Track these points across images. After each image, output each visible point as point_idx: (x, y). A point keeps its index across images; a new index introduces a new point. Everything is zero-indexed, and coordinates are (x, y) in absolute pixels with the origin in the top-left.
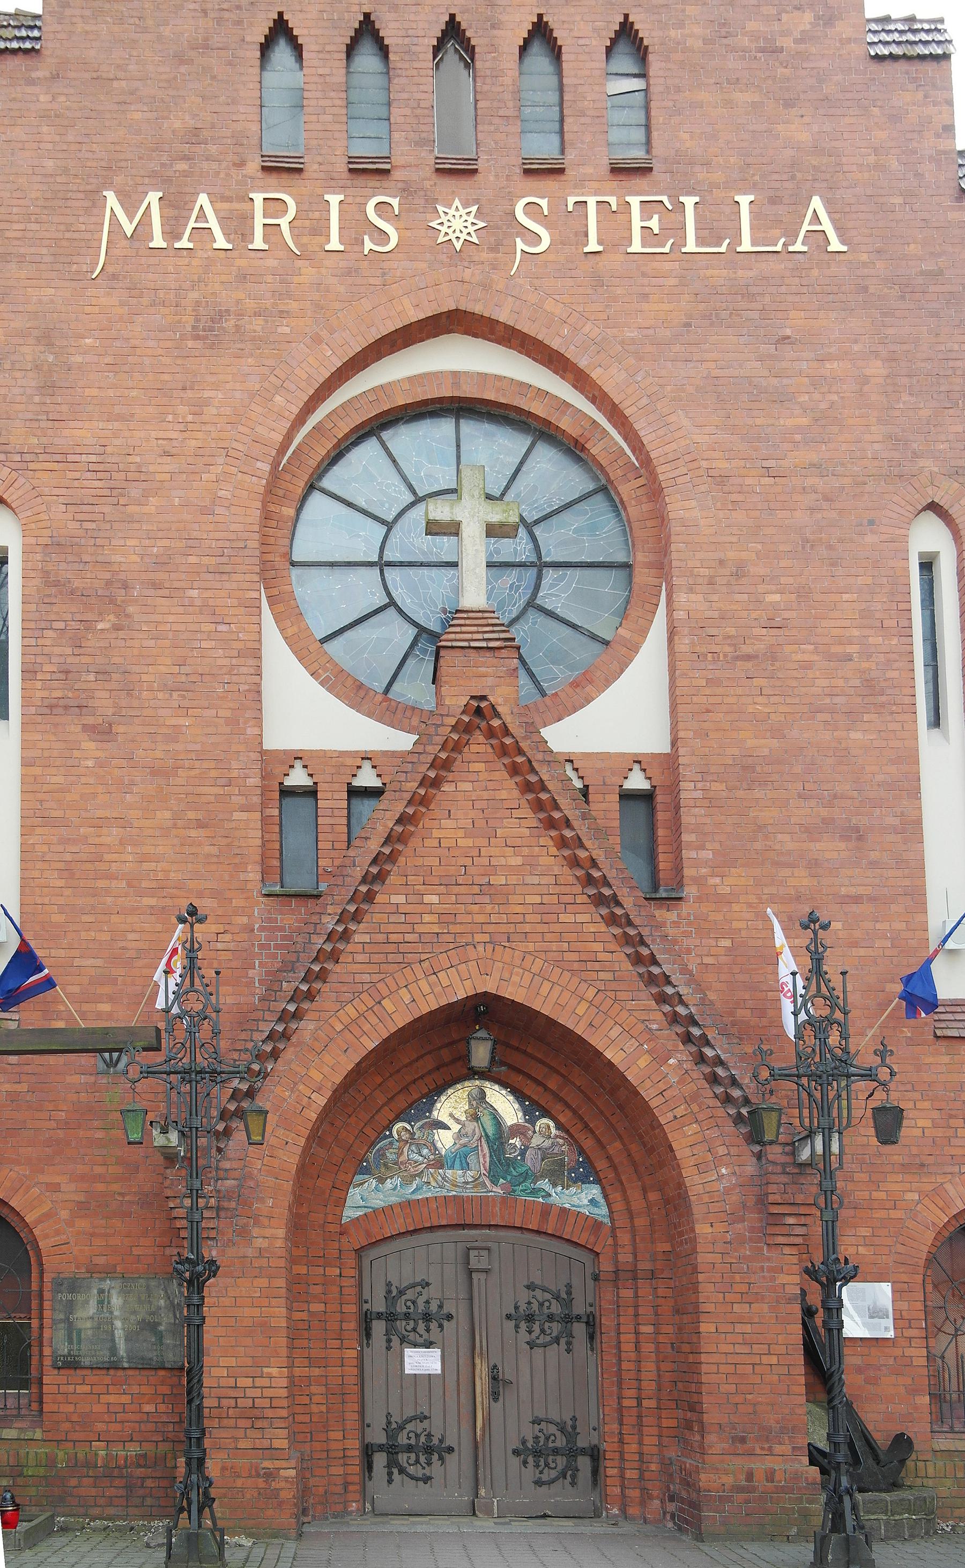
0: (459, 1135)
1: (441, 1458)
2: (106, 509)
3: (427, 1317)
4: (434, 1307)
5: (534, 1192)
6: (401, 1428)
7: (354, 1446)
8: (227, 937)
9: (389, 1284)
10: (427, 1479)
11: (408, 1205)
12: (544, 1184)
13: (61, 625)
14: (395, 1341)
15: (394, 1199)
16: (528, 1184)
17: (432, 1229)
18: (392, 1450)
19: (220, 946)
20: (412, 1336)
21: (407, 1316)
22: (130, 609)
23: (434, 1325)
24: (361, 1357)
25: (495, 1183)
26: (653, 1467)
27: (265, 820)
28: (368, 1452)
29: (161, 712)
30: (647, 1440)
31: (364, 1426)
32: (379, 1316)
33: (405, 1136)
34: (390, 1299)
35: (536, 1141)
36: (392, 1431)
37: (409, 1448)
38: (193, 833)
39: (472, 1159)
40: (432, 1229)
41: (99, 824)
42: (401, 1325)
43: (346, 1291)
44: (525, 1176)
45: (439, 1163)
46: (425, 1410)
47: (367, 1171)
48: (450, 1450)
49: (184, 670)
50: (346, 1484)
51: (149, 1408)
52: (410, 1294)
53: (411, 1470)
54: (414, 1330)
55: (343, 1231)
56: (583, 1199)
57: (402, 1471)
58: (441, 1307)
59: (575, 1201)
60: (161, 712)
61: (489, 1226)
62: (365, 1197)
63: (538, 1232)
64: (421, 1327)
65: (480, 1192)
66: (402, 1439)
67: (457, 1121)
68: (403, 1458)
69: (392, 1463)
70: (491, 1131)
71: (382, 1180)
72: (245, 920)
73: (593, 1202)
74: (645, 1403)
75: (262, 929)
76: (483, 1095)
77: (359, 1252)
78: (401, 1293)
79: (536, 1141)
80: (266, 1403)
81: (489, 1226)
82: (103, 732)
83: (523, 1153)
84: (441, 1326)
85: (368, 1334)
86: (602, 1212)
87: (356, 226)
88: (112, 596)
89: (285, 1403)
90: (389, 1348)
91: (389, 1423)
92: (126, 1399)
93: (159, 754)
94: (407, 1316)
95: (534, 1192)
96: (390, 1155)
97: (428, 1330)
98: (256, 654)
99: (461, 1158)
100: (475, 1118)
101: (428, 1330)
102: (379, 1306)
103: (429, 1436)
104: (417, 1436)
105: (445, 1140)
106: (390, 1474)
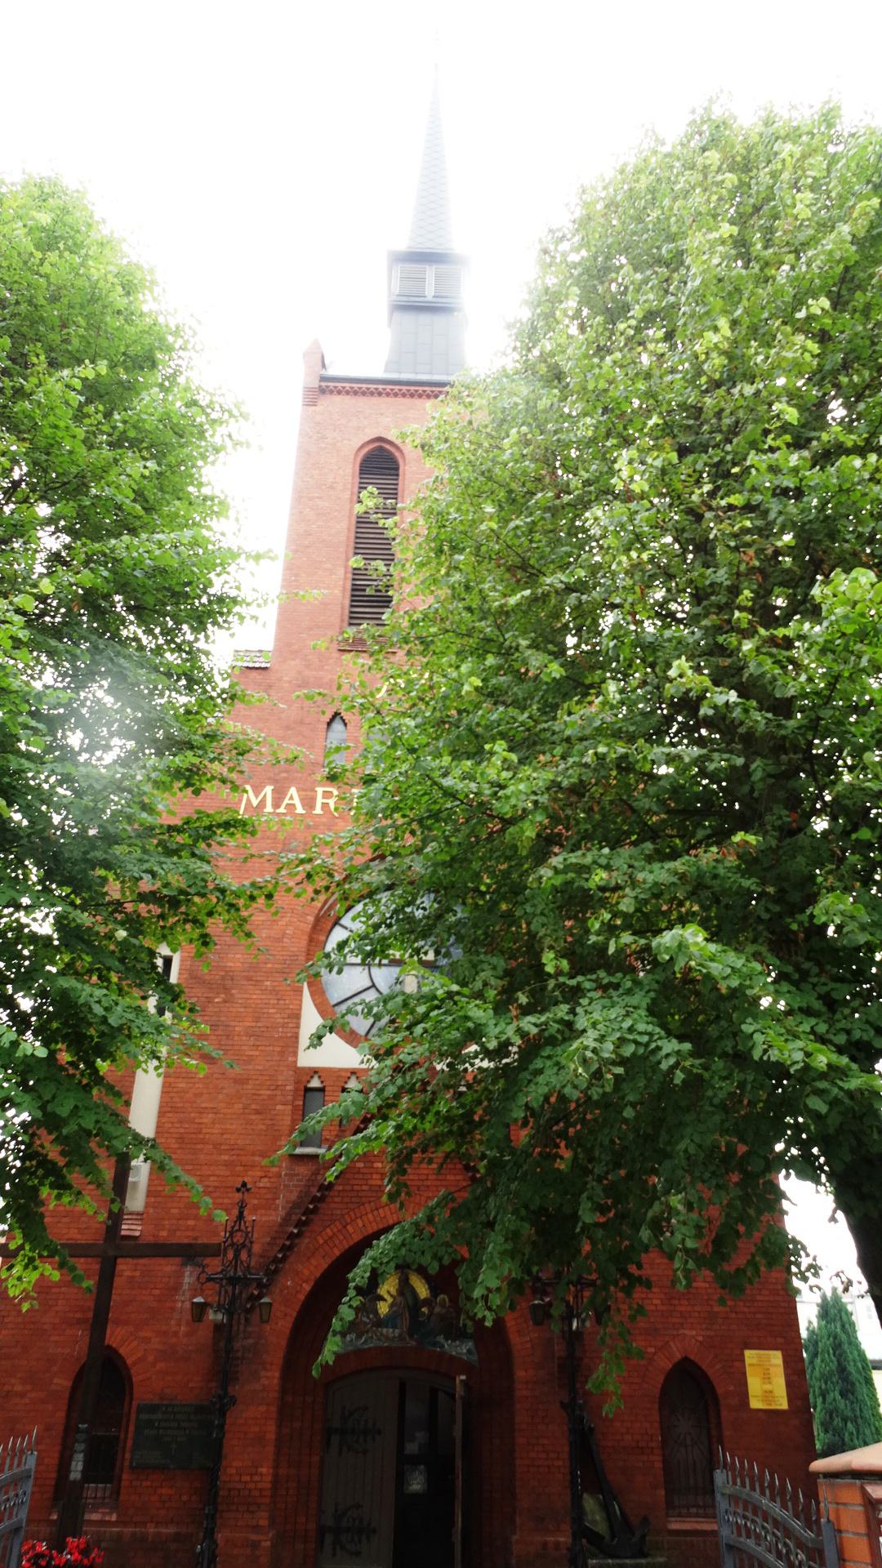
0: (391, 1306)
5: (435, 1344)
10: (358, 1554)
11: (359, 1353)
12: (441, 1339)
25: (411, 1336)
27: (295, 1108)
28: (322, 1531)
35: (437, 1309)
45: (380, 1323)
48: (374, 1531)
70: (410, 1302)
76: (407, 1279)
79: (437, 1309)
80: (257, 1493)
86: (474, 1358)
89: (268, 1493)
99: (392, 1320)
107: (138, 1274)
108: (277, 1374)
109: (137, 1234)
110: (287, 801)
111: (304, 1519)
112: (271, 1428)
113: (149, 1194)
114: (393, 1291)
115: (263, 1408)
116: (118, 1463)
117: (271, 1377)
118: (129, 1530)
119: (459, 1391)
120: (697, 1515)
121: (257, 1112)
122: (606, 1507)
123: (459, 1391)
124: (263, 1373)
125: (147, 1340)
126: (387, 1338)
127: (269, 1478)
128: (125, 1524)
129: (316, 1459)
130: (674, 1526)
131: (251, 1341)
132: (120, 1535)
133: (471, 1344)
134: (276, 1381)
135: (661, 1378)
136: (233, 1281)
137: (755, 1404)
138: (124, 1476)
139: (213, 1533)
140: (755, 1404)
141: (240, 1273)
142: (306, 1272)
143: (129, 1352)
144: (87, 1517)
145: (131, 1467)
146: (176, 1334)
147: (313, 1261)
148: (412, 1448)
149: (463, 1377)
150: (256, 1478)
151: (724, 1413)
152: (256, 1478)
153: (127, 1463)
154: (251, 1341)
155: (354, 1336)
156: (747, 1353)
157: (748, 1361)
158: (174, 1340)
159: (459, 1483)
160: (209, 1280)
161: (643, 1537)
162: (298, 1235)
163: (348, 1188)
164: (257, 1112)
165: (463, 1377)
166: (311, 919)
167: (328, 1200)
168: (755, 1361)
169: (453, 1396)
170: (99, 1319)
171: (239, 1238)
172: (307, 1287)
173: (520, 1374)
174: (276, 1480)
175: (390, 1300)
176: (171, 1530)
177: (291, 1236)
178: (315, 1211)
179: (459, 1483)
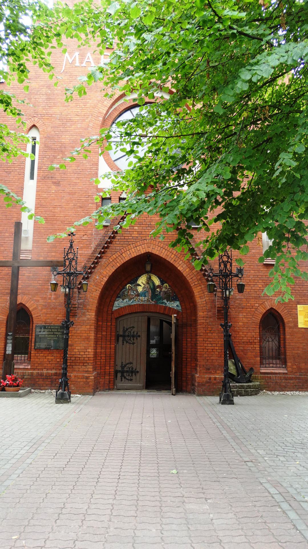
0: (144, 288)
1: (135, 374)
2: (61, 128)
3: (133, 336)
4: (135, 333)
5: (163, 303)
6: (125, 366)
7: (112, 370)
8: (86, 236)
9: (124, 327)
10: (131, 380)
11: (130, 306)
12: (165, 301)
13: (48, 157)
14: (125, 342)
15: (126, 305)
16: (161, 301)
17: (136, 313)
18: (122, 372)
19: (84, 238)
20: (129, 341)
21: (128, 336)
22: (66, 153)
23: (135, 338)
24: (115, 347)
25: (152, 300)
26: (189, 377)
28: (116, 372)
29: (72, 179)
30: (188, 369)
31: (115, 365)
32: (121, 336)
33: (130, 288)
34: (124, 331)
35: (163, 289)
36: (123, 367)
37: (127, 372)
38: (79, 209)
39: (147, 294)
40: (136, 313)
41: (55, 207)
42: (127, 338)
43: (112, 329)
44: (160, 299)
45: (138, 295)
46: (131, 360)
47: (120, 297)
48: (138, 372)
49: (79, 168)
50: (109, 382)
51: (58, 360)
52: (129, 330)
53: (127, 377)
54: (130, 340)
55: (112, 313)
56: (175, 305)
57: (125, 378)
58: (137, 333)
59: (173, 305)
60: (72, 179)
61: (150, 312)
62: (119, 304)
63: (163, 314)
64: (132, 339)
65: (149, 303)
66: (125, 369)
67: (144, 284)
68: (125, 374)
69: (122, 376)
70: (152, 287)
71: (123, 300)
72: (90, 232)
73: (177, 306)
74: (188, 359)
75: (95, 234)
76: (150, 277)
77: (117, 319)
78: (127, 329)
79: (163, 289)
81: (150, 312)
82: (57, 183)
83: (160, 293)
84: (137, 339)
85: (118, 341)
86: (180, 308)
88: (62, 150)
90: (123, 344)
91: (122, 365)
92: (52, 358)
93: (71, 189)
94: (128, 336)
95: (163, 303)
96: (126, 293)
97: (133, 340)
98: (97, 164)
99: (144, 294)
100: (148, 283)
101: (133, 340)
102: (121, 333)
103: (132, 368)
104: (129, 368)
105: (140, 289)
106: (122, 378)
107: (31, 275)
108: (94, 314)
109: (30, 258)
110: (86, 60)
111: (108, 368)
112: (92, 335)
113: (34, 242)
114: (144, 283)
115: (88, 327)
116: (30, 347)
117: (91, 315)
118: (35, 372)
119: (174, 321)
120: (273, 367)
121: (80, 207)
122: (235, 364)
123: (174, 321)
124: (87, 313)
125: (38, 301)
126: (142, 301)
127: (92, 353)
128: (34, 369)
129: (113, 346)
130: (263, 371)
131: (81, 301)
132: (32, 373)
133: (178, 303)
134: (93, 317)
135: (261, 316)
136: (69, 274)
137: (300, 325)
138: (32, 352)
139: (66, 374)
140: (300, 325)
141: (72, 271)
142: (105, 273)
143: (30, 305)
144: (15, 367)
145: (34, 349)
146: (50, 298)
147: (108, 268)
148: (153, 342)
149: (175, 315)
150: (86, 353)
151: (287, 329)
152: (86, 353)
153: (33, 347)
154: (81, 301)
155: (128, 300)
156: (299, 306)
157: (299, 309)
158: (49, 301)
159: (173, 355)
160: (58, 274)
161: (251, 375)
162: (100, 258)
163: (123, 238)
164: (80, 207)
165: (175, 315)
166: (101, 119)
167: (114, 243)
168: (302, 309)
169: (170, 324)
170: (14, 292)
171: (71, 256)
172: (106, 279)
173: (200, 314)
174: (96, 354)
175: (143, 286)
176: (54, 371)
177: (97, 258)
178: (107, 247)
179: (173, 355)
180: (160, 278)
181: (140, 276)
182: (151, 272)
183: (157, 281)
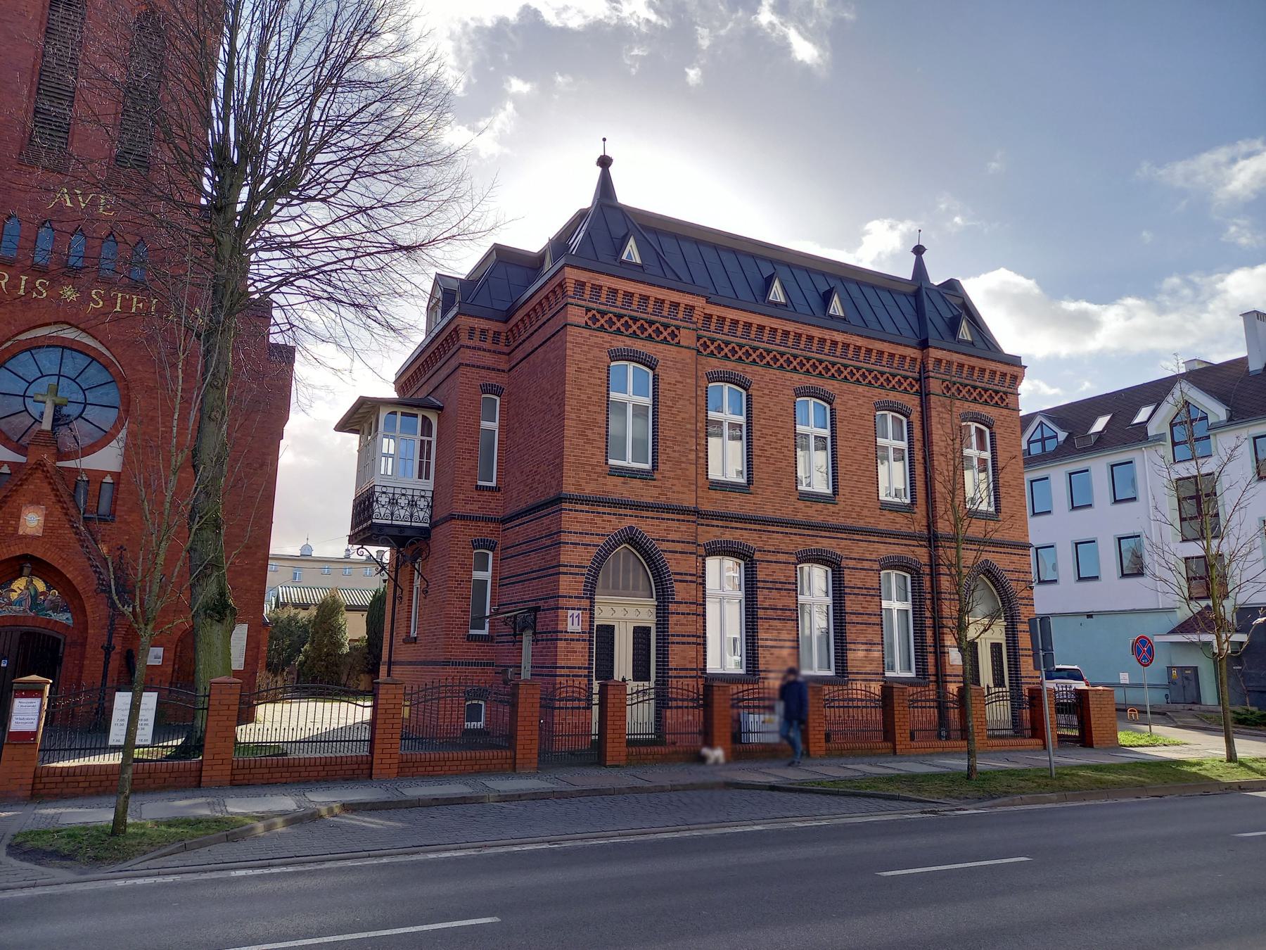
12: (50, 612)
45: (10, 603)
56: (64, 617)
87: (31, 288)
99: (19, 602)
105: (14, 596)
180: (45, 582)
181: (16, 578)
182: (31, 574)
183: (40, 585)
